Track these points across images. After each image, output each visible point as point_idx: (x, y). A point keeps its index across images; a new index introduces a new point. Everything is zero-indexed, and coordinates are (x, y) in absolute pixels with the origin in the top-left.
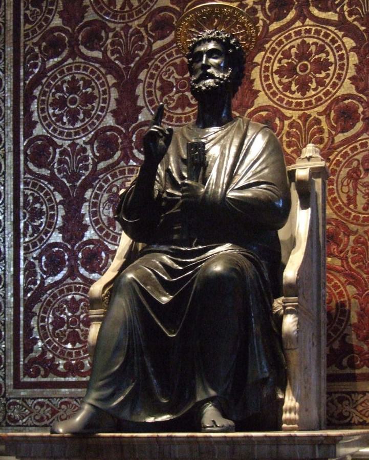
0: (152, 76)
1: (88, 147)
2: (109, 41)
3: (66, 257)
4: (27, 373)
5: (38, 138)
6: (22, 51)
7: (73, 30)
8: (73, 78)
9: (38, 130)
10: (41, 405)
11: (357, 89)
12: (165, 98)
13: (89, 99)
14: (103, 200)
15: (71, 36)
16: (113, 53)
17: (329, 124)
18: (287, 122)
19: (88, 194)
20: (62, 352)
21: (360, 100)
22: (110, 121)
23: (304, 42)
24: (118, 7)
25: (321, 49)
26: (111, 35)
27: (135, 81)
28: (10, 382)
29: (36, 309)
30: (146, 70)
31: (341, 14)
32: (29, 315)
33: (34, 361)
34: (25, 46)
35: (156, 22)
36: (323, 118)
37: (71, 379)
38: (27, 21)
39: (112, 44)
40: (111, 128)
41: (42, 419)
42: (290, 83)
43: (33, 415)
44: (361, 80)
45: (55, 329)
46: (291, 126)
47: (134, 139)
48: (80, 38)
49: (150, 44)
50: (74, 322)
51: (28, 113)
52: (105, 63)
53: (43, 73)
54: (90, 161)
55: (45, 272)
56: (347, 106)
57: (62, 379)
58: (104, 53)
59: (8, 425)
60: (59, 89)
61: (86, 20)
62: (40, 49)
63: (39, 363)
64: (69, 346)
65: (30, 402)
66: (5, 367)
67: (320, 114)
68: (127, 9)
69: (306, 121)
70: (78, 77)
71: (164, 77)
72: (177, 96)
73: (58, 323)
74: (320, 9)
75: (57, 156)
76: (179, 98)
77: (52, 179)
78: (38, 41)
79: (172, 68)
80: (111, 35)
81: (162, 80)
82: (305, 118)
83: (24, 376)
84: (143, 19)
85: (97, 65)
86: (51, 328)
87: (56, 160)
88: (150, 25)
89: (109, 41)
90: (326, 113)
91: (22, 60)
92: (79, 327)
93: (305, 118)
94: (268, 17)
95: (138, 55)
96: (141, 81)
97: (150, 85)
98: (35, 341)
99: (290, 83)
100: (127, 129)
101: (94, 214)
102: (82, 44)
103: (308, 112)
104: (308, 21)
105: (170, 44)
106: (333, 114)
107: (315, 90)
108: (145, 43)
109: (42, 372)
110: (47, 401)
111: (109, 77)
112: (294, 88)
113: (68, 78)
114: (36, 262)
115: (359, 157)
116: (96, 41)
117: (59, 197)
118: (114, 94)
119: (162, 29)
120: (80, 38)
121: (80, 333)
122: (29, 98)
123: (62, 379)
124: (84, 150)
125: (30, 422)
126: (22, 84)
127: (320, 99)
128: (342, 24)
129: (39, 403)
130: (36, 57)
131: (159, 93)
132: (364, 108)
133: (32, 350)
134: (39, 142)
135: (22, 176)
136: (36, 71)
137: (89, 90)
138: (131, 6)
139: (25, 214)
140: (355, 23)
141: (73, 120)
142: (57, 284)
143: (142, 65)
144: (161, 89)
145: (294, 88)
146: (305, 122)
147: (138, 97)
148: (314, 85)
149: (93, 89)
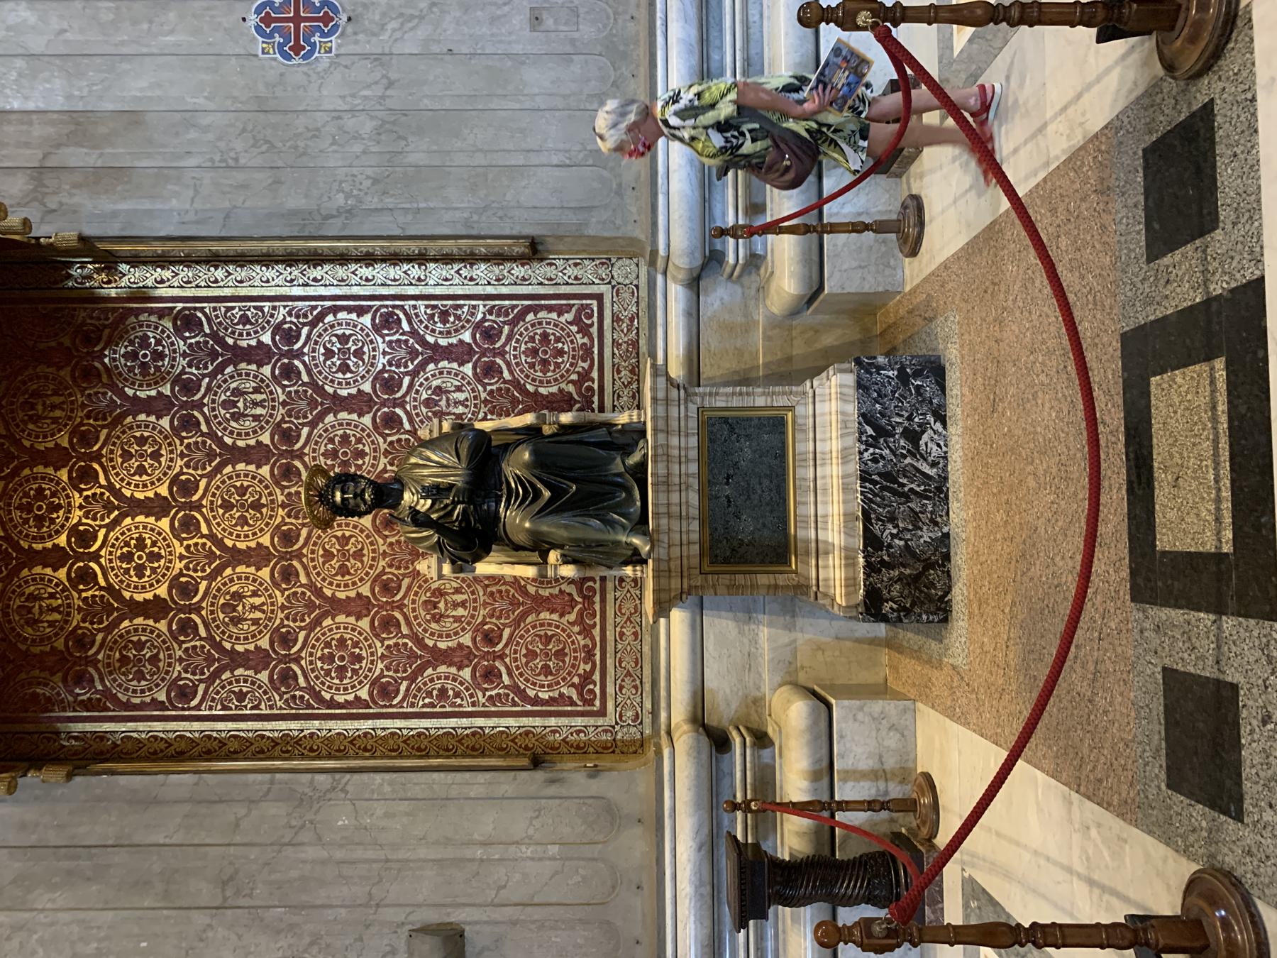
0: (331, 584)
1: (386, 643)
2: (292, 624)
3: (486, 663)
4: (590, 702)
5: (371, 694)
6: (285, 712)
7: (274, 659)
8: (320, 659)
9: (364, 694)
10: (621, 687)
11: (368, 413)
12: (352, 571)
13: (342, 642)
14: (438, 628)
15: (280, 662)
16: (303, 620)
17: (394, 434)
18: (389, 468)
19: (430, 643)
20: (573, 666)
21: (378, 410)
22: (364, 623)
23: (323, 455)
24: (263, 616)
25: (331, 441)
26: (286, 622)
27: (333, 600)
28: (600, 721)
29: (531, 693)
30: (324, 590)
31: (304, 425)
32: (536, 701)
33: (580, 694)
34: (281, 708)
35: (282, 580)
36: (389, 439)
37: (598, 658)
38: (256, 707)
39: (295, 621)
40: (372, 622)
41: (635, 687)
42: (356, 465)
43: (632, 697)
44: (361, 409)
45: (551, 674)
46: (392, 464)
47: (384, 600)
48: (283, 652)
49: (301, 586)
50: (547, 655)
51: (347, 704)
52: (311, 628)
53: (310, 689)
54: (400, 641)
55: (498, 685)
56: (382, 420)
57: (598, 666)
58: (301, 628)
59: (641, 723)
60: (328, 673)
61: (268, 648)
62: (286, 693)
63: (583, 690)
64: (567, 659)
65: (619, 700)
66: (585, 727)
67: (385, 442)
68: (265, 608)
69: (391, 453)
70: (319, 654)
71: (334, 572)
72: (352, 561)
73: (546, 670)
74: (297, 441)
75: (391, 673)
76: (355, 559)
77: (412, 679)
78: (279, 695)
79: (327, 565)
80: (286, 622)
81: (336, 574)
82: (387, 453)
83: (594, 705)
84: (277, 592)
85: (312, 635)
86: (550, 678)
87: (394, 675)
88: (284, 586)
89: (292, 624)
90: (384, 436)
91: (294, 711)
92: (551, 650)
93: (387, 453)
94: (297, 483)
95: (309, 597)
96: (333, 594)
97: (338, 586)
98: (561, 695)
99: (356, 465)
100: (374, 606)
101: (448, 636)
102: (289, 650)
103: (382, 451)
104: (306, 451)
105: (305, 567)
106: (387, 432)
107: (364, 445)
108: (299, 590)
109: (591, 687)
110: (618, 682)
111: (324, 624)
112: (360, 462)
113: (319, 664)
114: (488, 694)
115: (424, 410)
116: (289, 637)
117: (430, 671)
118: (341, 618)
119: (290, 575)
120: (283, 652)
121: (557, 648)
122: (332, 704)
123: (598, 666)
124: (388, 647)
125: (639, 700)
126: (316, 711)
127: (373, 442)
128: (313, 425)
129: (621, 690)
130: (294, 697)
131: (347, 577)
132: (385, 406)
133: (570, 698)
134: (375, 692)
135: (405, 710)
136: (307, 697)
137: (334, 643)
138: (263, 604)
139: (441, 707)
140: (314, 413)
141: (359, 658)
142: (510, 674)
143: (319, 592)
144: (343, 576)
145: (360, 462)
146: (391, 453)
147: (347, 597)
148: (360, 446)
149: (333, 639)
